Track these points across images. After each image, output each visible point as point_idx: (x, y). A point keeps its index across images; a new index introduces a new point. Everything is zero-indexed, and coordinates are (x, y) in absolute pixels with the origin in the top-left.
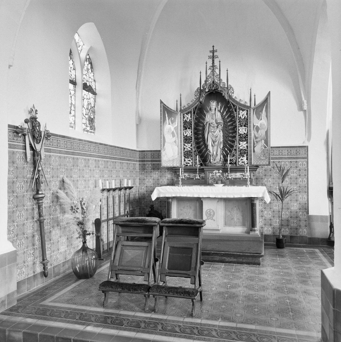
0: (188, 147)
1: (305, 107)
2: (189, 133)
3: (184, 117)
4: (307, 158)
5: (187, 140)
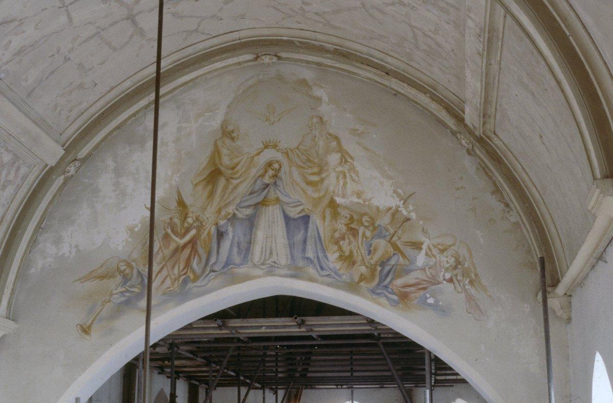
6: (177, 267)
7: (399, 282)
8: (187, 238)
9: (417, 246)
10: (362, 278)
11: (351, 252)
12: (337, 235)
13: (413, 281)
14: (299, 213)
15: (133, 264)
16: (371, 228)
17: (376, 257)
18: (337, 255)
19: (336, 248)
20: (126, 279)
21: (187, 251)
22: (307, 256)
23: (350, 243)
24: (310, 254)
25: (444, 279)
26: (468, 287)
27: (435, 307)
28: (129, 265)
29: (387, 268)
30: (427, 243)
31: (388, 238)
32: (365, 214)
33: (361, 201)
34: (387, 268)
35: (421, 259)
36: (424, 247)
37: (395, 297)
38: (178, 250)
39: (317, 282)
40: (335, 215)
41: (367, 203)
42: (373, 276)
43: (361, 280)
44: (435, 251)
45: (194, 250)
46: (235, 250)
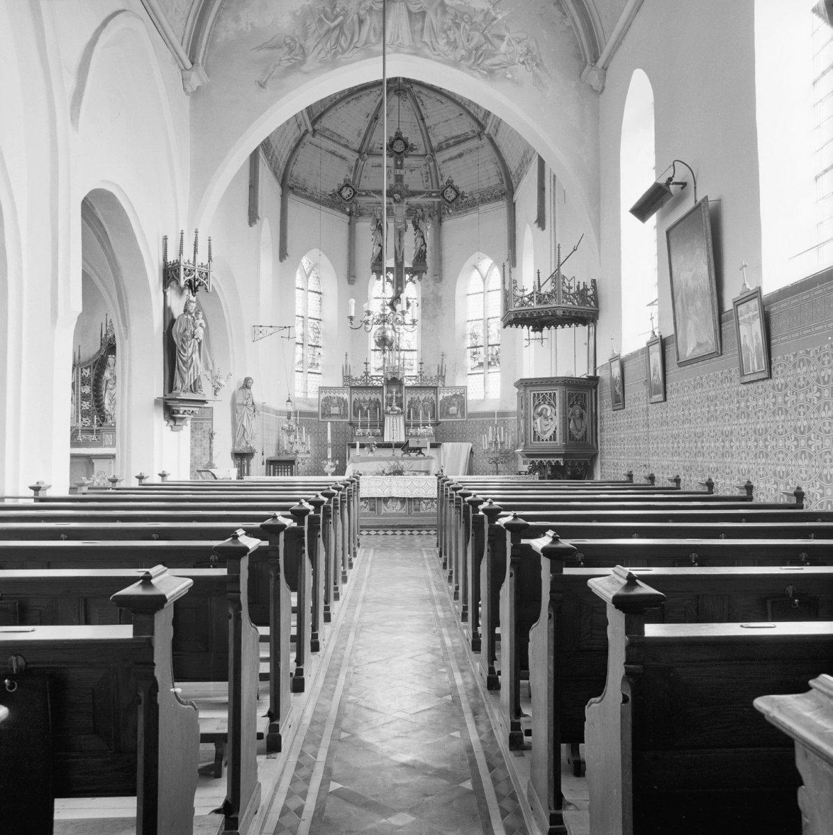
0: (86, 405)
1: (211, 367)
2: (87, 390)
3: (82, 372)
4: (212, 419)
5: (85, 397)
6: (329, 43)
7: (488, 62)
8: (336, 22)
9: (501, 38)
10: (463, 58)
11: (455, 39)
12: (445, 27)
13: (498, 62)
14: (419, 9)
15: (296, 39)
16: (469, 24)
17: (473, 44)
18: (445, 41)
19: (444, 36)
20: (291, 50)
21: (337, 32)
22: (423, 40)
23: (454, 34)
24: (426, 39)
25: (519, 62)
26: (535, 68)
27: (512, 80)
28: (293, 40)
29: (480, 52)
30: (508, 36)
31: (481, 31)
32: (465, 13)
33: (463, 4)
34: (480, 52)
35: (503, 47)
36: (506, 39)
37: (485, 72)
38: (330, 31)
39: (430, 58)
40: (445, 12)
41: (467, 5)
42: (470, 58)
43: (461, 60)
44: (513, 42)
45: (342, 32)
46: (372, 33)
